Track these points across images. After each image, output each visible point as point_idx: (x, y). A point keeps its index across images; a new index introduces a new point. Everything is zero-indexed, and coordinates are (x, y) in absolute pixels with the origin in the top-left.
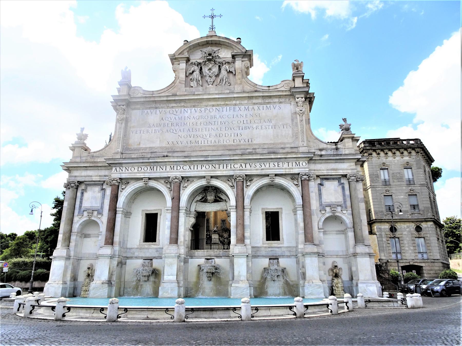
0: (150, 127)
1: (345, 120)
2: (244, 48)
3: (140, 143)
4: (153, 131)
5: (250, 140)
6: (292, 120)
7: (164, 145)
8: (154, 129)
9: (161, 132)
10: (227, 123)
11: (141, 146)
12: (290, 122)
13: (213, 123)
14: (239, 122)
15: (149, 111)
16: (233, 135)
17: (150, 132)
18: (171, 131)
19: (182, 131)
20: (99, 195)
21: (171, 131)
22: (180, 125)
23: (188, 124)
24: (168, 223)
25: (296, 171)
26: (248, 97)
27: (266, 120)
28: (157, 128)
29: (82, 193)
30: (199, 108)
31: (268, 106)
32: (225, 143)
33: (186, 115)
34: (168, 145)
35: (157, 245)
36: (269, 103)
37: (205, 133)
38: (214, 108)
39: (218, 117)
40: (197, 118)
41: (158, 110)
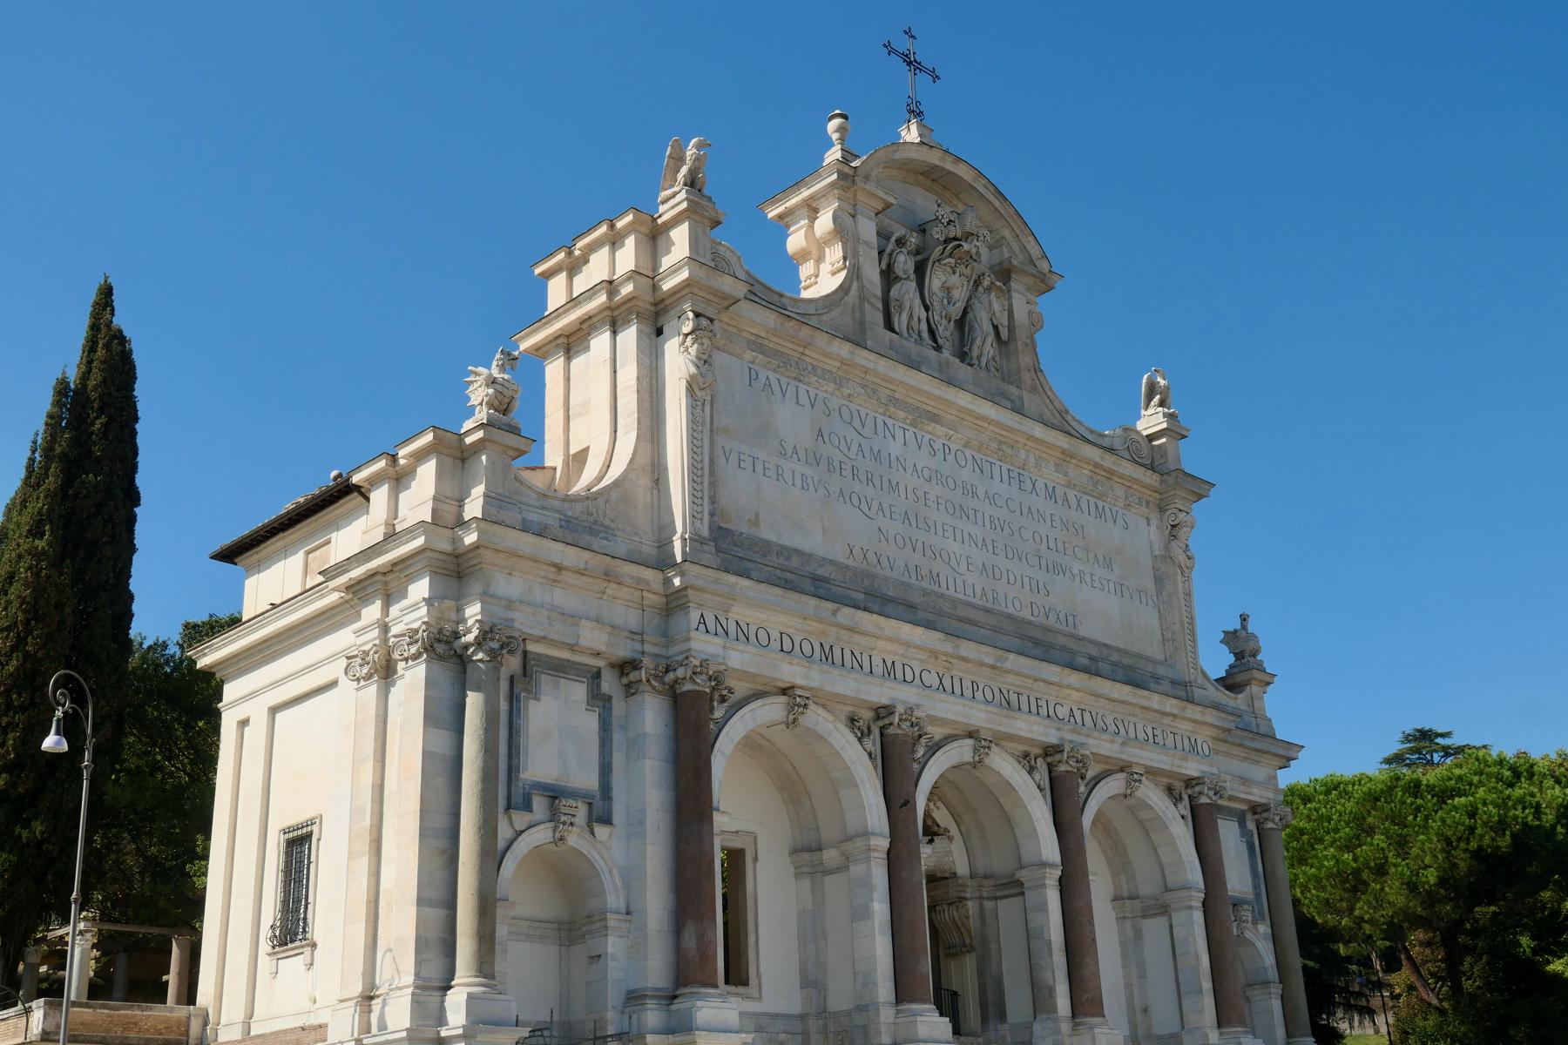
0: (783, 454)
1: (1244, 618)
2: (1045, 256)
3: (757, 516)
4: (798, 481)
5: (1070, 619)
6: (1159, 580)
7: (838, 553)
8: (801, 468)
9: (822, 491)
10: (1007, 530)
11: (765, 533)
12: (1150, 584)
13: (971, 513)
14: (1037, 537)
15: (772, 375)
16: (1026, 580)
17: (788, 475)
18: (855, 500)
19: (888, 514)
20: (591, 722)
21: (855, 500)
22: (877, 482)
23: (902, 486)
24: (880, 908)
25: (1192, 768)
26: (1063, 452)
27: (1101, 559)
28: (808, 471)
29: (512, 698)
30: (927, 437)
31: (1100, 504)
32: (1011, 610)
33: (895, 448)
34: (850, 562)
35: (750, 998)
36: (1101, 496)
37: (955, 547)
38: (968, 452)
39: (981, 493)
40: (926, 473)
41: (802, 387)
